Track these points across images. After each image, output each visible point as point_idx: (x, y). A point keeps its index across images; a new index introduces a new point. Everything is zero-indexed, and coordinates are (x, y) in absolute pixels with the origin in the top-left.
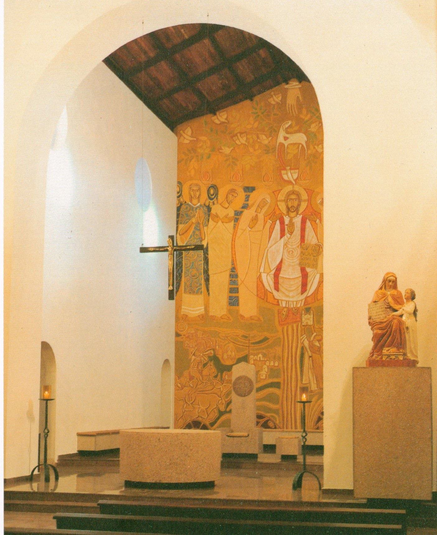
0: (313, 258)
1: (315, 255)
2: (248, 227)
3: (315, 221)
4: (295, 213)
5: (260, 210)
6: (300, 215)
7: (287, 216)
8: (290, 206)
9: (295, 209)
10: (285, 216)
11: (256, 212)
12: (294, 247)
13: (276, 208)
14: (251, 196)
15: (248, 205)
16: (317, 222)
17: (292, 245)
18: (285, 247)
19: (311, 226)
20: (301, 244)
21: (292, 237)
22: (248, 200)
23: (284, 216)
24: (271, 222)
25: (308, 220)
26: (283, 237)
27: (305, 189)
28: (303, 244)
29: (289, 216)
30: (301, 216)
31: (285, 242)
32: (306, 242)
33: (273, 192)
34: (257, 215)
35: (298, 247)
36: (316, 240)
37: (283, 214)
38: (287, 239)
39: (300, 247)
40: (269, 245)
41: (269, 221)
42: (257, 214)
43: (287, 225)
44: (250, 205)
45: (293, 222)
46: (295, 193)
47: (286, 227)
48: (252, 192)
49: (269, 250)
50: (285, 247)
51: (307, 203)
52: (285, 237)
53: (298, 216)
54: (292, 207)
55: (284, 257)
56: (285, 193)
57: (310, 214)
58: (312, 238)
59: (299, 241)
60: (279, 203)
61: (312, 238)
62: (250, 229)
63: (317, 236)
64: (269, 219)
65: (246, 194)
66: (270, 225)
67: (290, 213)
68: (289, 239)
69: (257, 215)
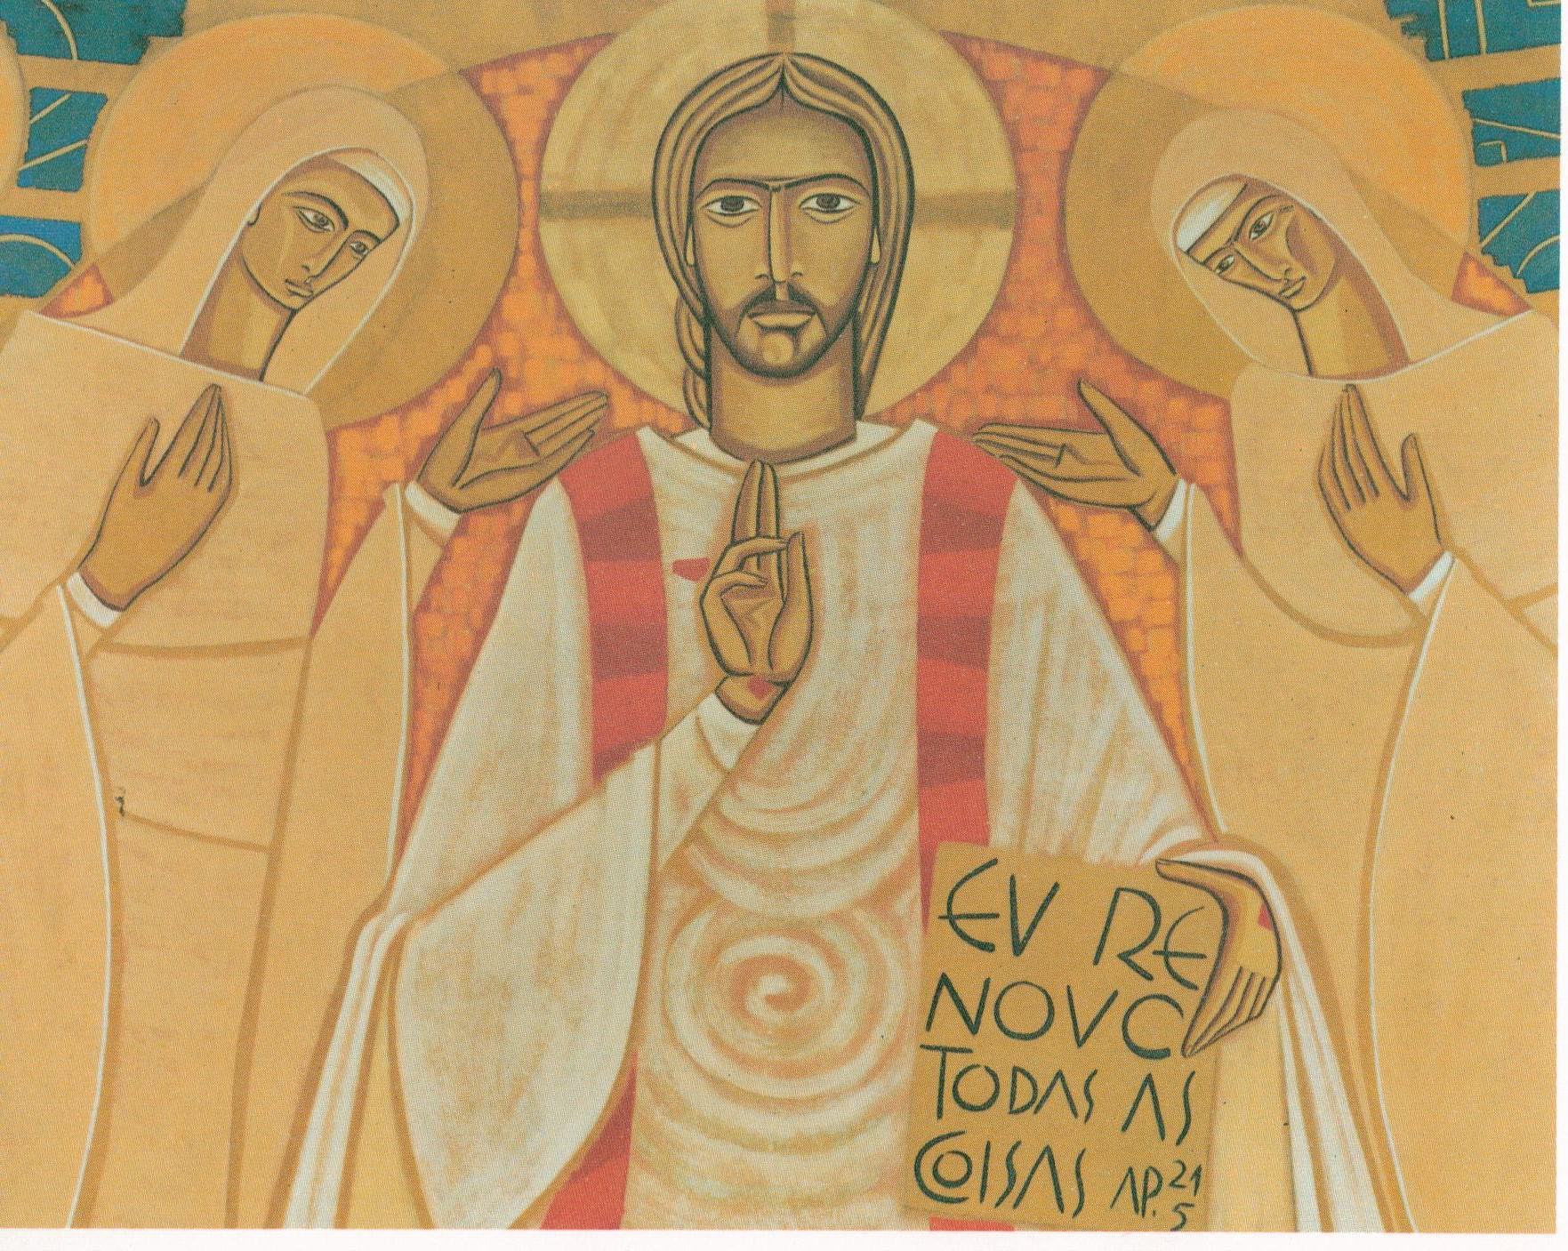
0: (1125, 1073)
1: (1155, 1026)
2: (76, 580)
3: (1142, 517)
4: (824, 385)
5: (263, 321)
6: (897, 419)
7: (699, 439)
8: (731, 292)
9: (814, 334)
10: (669, 437)
11: (197, 350)
12: (819, 903)
13: (523, 306)
14: (109, 125)
15: (70, 236)
16: (1164, 532)
17: (779, 883)
18: (674, 897)
19: (1075, 593)
20: (926, 858)
21: (775, 750)
22: (68, 176)
23: (647, 437)
24: (445, 521)
25: (1022, 500)
26: (643, 758)
27: (960, 43)
28: (954, 859)
29: (723, 441)
30: (922, 434)
31: (674, 829)
32: (1001, 835)
33: (471, 76)
34: (215, 400)
35: (880, 899)
36: (1173, 801)
37: (640, 395)
38: (704, 782)
39: (908, 901)
40: (414, 876)
41: (417, 497)
42: (215, 393)
43: (686, 569)
44: (98, 242)
45: (793, 520)
46: (801, 86)
47: (682, 592)
48: (134, 49)
49: (424, 937)
50: (674, 897)
51: (998, 242)
52: (679, 740)
53: (868, 433)
54: (763, 300)
55: (655, 1056)
56: (667, 92)
57: (1059, 406)
58: (1110, 761)
59: (886, 809)
60: (553, 236)
61: (1110, 761)
62: (107, 617)
63: (1175, 738)
64: (419, 470)
65: (48, 72)
66: (428, 556)
67: (728, 372)
68: (730, 779)
69: (215, 400)
